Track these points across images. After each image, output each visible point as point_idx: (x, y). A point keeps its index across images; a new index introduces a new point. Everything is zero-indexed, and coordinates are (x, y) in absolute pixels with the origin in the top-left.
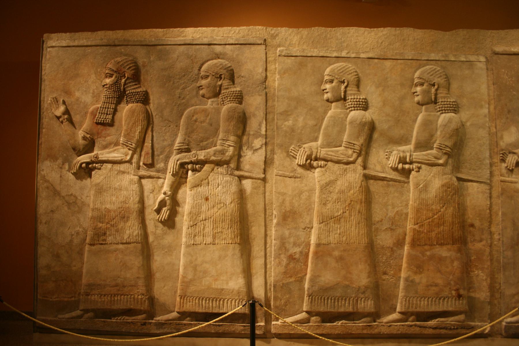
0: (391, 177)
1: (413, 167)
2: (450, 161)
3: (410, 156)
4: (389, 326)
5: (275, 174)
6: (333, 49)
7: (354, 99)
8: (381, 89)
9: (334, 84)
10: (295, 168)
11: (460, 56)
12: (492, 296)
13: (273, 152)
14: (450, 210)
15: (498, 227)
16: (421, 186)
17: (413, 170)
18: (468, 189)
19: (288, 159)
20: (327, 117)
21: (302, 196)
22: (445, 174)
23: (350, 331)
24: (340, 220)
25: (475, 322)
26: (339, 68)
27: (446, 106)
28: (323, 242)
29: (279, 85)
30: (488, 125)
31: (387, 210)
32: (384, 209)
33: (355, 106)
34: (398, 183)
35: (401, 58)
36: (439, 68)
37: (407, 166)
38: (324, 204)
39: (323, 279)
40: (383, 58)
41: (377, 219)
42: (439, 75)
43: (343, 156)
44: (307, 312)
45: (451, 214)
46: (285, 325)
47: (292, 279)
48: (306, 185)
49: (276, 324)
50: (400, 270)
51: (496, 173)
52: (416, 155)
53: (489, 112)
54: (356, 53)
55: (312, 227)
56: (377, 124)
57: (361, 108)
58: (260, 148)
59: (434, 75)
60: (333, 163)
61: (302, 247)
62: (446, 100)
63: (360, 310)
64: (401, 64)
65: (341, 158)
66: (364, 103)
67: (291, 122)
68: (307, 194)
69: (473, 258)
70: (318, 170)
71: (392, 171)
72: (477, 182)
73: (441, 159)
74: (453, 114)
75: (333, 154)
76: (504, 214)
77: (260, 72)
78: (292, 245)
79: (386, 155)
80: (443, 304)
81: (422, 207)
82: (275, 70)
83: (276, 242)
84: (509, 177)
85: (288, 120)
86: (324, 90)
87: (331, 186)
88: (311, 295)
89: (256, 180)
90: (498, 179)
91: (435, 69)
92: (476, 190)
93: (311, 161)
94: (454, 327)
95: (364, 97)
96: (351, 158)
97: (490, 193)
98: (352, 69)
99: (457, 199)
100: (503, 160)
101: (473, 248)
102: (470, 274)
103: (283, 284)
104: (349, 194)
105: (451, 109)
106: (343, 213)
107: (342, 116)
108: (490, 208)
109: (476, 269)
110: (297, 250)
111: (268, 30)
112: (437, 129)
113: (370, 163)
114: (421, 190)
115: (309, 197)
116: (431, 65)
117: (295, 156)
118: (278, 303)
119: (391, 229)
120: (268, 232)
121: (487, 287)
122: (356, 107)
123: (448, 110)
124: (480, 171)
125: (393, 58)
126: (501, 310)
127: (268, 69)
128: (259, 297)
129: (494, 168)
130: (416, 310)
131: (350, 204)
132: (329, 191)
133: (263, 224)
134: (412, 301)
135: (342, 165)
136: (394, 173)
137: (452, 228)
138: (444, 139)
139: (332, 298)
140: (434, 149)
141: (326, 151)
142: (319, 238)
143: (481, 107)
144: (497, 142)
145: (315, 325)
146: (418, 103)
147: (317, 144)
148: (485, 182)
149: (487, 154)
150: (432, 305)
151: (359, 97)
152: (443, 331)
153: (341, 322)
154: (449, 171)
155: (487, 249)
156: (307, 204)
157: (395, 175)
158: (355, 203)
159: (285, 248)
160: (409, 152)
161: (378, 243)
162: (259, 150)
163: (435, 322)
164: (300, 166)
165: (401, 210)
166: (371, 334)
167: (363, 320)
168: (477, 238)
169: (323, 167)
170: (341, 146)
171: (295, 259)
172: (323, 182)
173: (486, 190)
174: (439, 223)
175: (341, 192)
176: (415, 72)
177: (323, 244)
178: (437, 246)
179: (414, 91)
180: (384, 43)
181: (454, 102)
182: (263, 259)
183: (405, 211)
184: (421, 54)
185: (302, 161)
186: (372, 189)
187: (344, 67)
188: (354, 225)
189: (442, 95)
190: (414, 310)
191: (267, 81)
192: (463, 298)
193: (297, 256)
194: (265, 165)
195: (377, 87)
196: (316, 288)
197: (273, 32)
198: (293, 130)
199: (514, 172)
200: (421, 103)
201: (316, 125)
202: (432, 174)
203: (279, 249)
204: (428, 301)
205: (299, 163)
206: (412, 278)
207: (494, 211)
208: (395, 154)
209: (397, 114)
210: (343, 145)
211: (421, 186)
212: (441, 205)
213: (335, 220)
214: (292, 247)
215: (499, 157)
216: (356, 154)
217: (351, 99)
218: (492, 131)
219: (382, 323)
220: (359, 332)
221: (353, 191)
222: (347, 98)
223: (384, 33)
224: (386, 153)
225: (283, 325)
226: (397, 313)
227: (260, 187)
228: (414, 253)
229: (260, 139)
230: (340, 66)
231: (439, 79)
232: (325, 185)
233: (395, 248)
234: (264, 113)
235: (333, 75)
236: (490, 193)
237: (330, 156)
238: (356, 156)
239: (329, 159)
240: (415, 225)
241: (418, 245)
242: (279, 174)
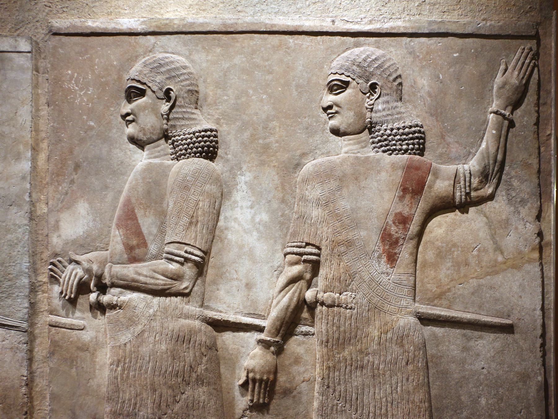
51: (43, 306)
76: (54, 397)
84: (67, 316)
100: (54, 279)
124: (9, 301)
148: (16, 327)
199: (78, 306)
207: (37, 389)
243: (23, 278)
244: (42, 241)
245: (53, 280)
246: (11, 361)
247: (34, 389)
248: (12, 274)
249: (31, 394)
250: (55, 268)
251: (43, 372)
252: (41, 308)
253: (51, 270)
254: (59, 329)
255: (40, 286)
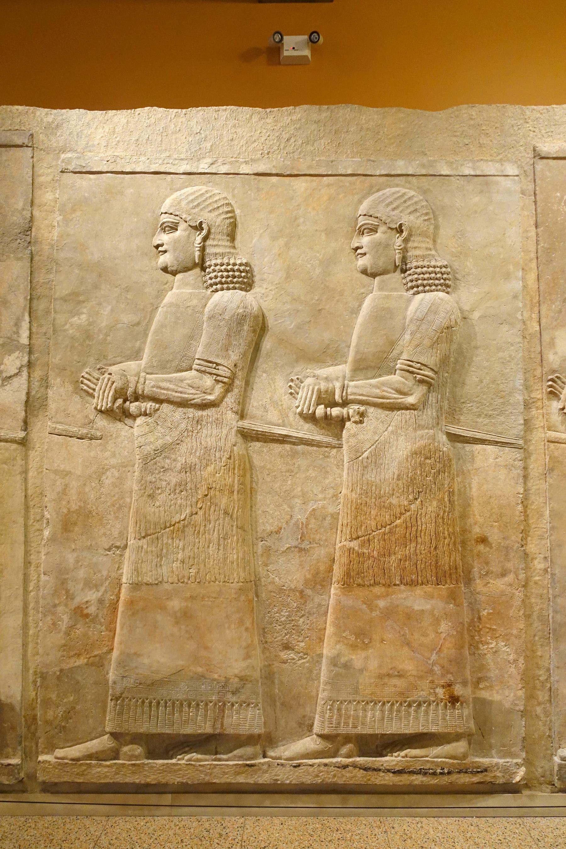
0: (300, 435)
1: (348, 413)
2: (432, 398)
3: (343, 387)
4: (295, 767)
5: (49, 430)
6: (182, 156)
7: (222, 265)
8: (282, 242)
9: (178, 233)
10: (92, 418)
11: (462, 165)
12: (530, 697)
13: (45, 383)
14: (432, 507)
15: (543, 542)
16: (366, 454)
17: (349, 420)
18: (473, 459)
19: (77, 398)
20: (162, 305)
21: (104, 477)
22: (420, 427)
23: (207, 778)
24: (183, 532)
25: (492, 757)
26: (191, 198)
27: (426, 276)
28: (148, 579)
29: (61, 236)
30: (520, 318)
31: (291, 508)
32: (285, 506)
33: (224, 280)
34: (315, 448)
35: (330, 173)
36: (412, 193)
37: (335, 411)
38: (149, 496)
39: (146, 661)
40: (288, 173)
41: (269, 528)
42: (412, 209)
43: (193, 391)
44: (112, 734)
45: (433, 515)
46: (61, 765)
47: (82, 661)
48: (114, 455)
49: (45, 762)
50: (321, 640)
51: (539, 422)
52: (356, 387)
53: (525, 287)
54: (231, 163)
55: (126, 546)
56: (271, 322)
57: (237, 285)
58: (16, 374)
59: (401, 209)
60: (171, 407)
61: (102, 589)
62: (426, 263)
63: (230, 731)
64: (329, 185)
65: (190, 394)
66: (243, 274)
67: (84, 317)
68: (117, 474)
69: (485, 613)
70: (140, 421)
71: (302, 422)
72: (496, 443)
73: (412, 394)
74: (441, 294)
75: (171, 386)
76: (554, 514)
77: (20, 209)
78: (81, 586)
79: (290, 387)
80: (416, 718)
81: (368, 500)
82: (52, 204)
83: (47, 578)
85: (79, 314)
86: (157, 247)
87: (165, 457)
88: (120, 697)
89: (8, 444)
90: (543, 435)
91: (404, 194)
92: (491, 460)
93: (125, 401)
94: (443, 769)
95: (244, 261)
96: (210, 394)
97: (525, 468)
98: (220, 199)
99: (446, 482)
101: (485, 590)
102: (478, 648)
103: (61, 671)
104: (205, 474)
105: (437, 282)
106: (192, 515)
107: (195, 302)
108: (525, 502)
109: (492, 638)
110: (92, 596)
111: (38, 113)
112: (404, 329)
113: (255, 404)
114: (365, 464)
115: (121, 480)
116: (397, 185)
117: (91, 391)
118: (50, 714)
119: (301, 550)
120: (33, 557)
121: (519, 678)
122: (226, 283)
123: (430, 286)
124: (502, 418)
125: (312, 173)
126: (550, 729)
127: (37, 201)
128: (9, 701)
129: (534, 412)
130: (354, 731)
131: (206, 495)
132: (163, 468)
133: (22, 539)
134: (347, 709)
135: (191, 410)
136: (307, 426)
137: (436, 548)
138: (419, 349)
139: (166, 703)
140: (398, 372)
141: (157, 380)
142: (136, 570)
143: (507, 276)
144: (541, 353)
145: (129, 765)
146: (364, 272)
147: (140, 365)
149: (519, 382)
150: (392, 719)
151: (232, 261)
152: (418, 780)
153: (188, 757)
154: (431, 420)
155: (517, 593)
156: (114, 496)
157: (309, 430)
158: (217, 493)
159: (67, 591)
160: (340, 379)
161: (269, 580)
162: (15, 379)
163: (399, 758)
164: (101, 411)
165: (323, 507)
166: (256, 784)
167: (235, 752)
168: (495, 568)
169: (150, 415)
170: (191, 369)
171: (87, 616)
172: (148, 449)
173: (514, 460)
174: (405, 537)
175: (188, 469)
176: (360, 202)
177: (147, 584)
178: (402, 587)
179: (357, 245)
180: (293, 140)
181: (446, 267)
182: (21, 616)
183: (331, 509)
184: (373, 161)
185: (106, 404)
186: (257, 461)
187: (202, 195)
188: (216, 541)
189: (418, 252)
190: (350, 730)
191: (33, 229)
192: (462, 704)
193: (92, 610)
194: (26, 411)
195: (274, 239)
196: (130, 682)
197: (50, 119)
198: (88, 336)
200: (369, 271)
201: (138, 324)
202: (390, 428)
203: (53, 595)
204: (382, 711)
205: (99, 408)
206: (346, 658)
207: (533, 507)
208: (309, 385)
209: (316, 298)
210: (195, 366)
211: (366, 454)
212: (411, 497)
213: (173, 532)
214: (82, 590)
215: (545, 387)
216: (221, 385)
217: (216, 265)
218: (531, 331)
219: (279, 758)
220: (228, 781)
221: (213, 466)
222: (208, 264)
223: (294, 118)
224: (291, 384)
225: (60, 764)
226: (315, 736)
227: (15, 459)
228: (350, 602)
229: (16, 354)
230: (192, 194)
231: (412, 217)
232: (152, 452)
233: (309, 592)
234: (25, 298)
235: (177, 213)
236: (525, 468)
237: (165, 392)
238: (222, 390)
239: (162, 397)
240: (352, 539)
241: (359, 585)
242: (56, 431)
243: (516, 395)
244: (535, 358)
245: (551, 396)
246: (505, 479)
247: (529, 507)
248: (504, 391)
249: (525, 512)
250: (554, 384)
251: (539, 489)
252: (536, 425)
253: (550, 386)
254: (559, 445)
255: (534, 402)
